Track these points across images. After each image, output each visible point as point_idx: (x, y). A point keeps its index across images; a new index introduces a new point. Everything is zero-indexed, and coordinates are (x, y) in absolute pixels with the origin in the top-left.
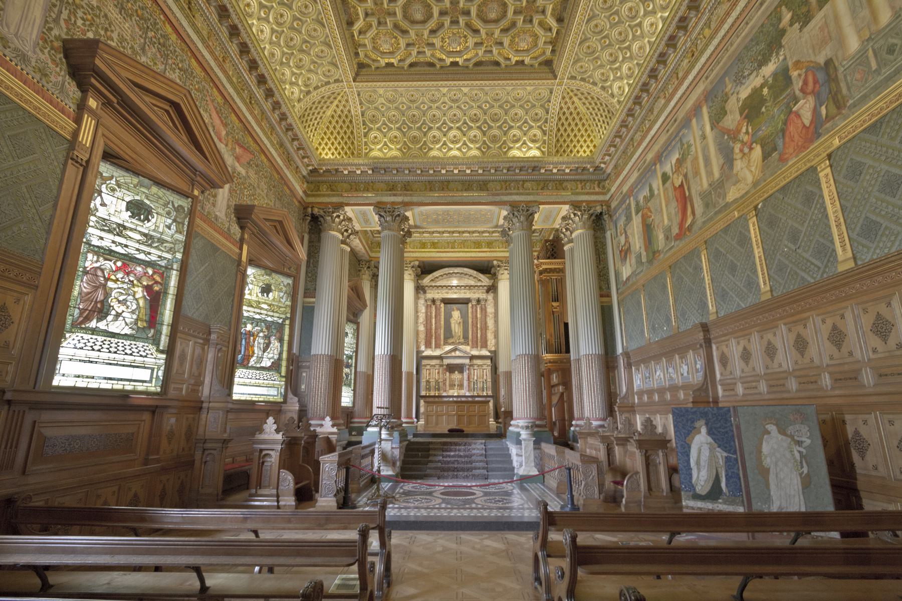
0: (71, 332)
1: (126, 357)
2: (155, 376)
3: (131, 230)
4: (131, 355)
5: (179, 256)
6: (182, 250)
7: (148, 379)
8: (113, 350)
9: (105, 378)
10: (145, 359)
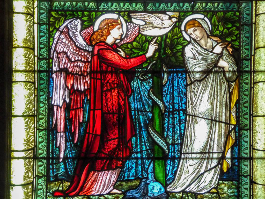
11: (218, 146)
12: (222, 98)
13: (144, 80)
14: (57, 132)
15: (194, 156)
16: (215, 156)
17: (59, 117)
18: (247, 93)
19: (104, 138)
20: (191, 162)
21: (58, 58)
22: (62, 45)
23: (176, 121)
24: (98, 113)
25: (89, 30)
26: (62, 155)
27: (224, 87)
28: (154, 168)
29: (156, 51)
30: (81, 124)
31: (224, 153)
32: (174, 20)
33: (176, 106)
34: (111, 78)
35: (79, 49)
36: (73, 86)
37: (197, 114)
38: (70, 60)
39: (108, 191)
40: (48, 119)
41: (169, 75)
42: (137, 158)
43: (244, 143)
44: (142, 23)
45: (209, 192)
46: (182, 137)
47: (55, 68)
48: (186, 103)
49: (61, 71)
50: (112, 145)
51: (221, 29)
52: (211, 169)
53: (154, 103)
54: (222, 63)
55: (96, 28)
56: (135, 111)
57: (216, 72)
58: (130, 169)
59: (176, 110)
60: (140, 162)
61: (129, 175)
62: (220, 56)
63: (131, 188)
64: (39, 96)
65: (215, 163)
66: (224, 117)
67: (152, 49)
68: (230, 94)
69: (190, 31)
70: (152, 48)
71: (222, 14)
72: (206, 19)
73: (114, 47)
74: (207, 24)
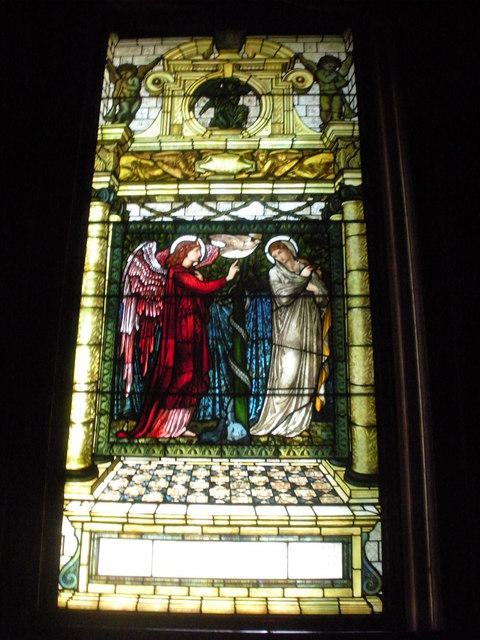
0: (109, 458)
2: (357, 562)
3: (216, 152)
4: (272, 502)
5: (353, 179)
6: (356, 161)
7: (338, 574)
9: (212, 583)
10: (320, 511)
11: (309, 380)
12: (311, 325)
13: (224, 305)
14: (124, 364)
15: (280, 392)
16: (306, 392)
17: (127, 345)
18: (340, 319)
19: (177, 371)
20: (277, 399)
21: (130, 282)
22: (134, 268)
23: (260, 352)
24: (171, 342)
25: (165, 253)
26: (128, 389)
27: (314, 313)
28: (234, 407)
29: (237, 274)
30: (151, 355)
31: (316, 389)
32: (257, 242)
33: (260, 334)
34: (187, 304)
35: (153, 272)
36: (144, 312)
37: (284, 343)
38: (142, 285)
39: (180, 432)
40: (116, 348)
41: (251, 300)
42: (214, 395)
43: (339, 377)
44: (222, 245)
45: (300, 435)
46: (267, 370)
47: (126, 292)
48: (271, 331)
49: (131, 296)
50: (187, 377)
51: (308, 251)
52: (301, 408)
53: (234, 330)
54: (311, 287)
55: (172, 251)
56: (213, 340)
57: (305, 297)
58: (206, 408)
59: (259, 339)
60: (218, 399)
61: (205, 414)
62: (309, 279)
63: (207, 430)
64: (107, 323)
65: (306, 400)
66: (315, 347)
67: (233, 271)
68: (322, 321)
69: (275, 253)
70: (233, 271)
71: (309, 235)
72: (292, 240)
73: (191, 270)
74: (294, 245)
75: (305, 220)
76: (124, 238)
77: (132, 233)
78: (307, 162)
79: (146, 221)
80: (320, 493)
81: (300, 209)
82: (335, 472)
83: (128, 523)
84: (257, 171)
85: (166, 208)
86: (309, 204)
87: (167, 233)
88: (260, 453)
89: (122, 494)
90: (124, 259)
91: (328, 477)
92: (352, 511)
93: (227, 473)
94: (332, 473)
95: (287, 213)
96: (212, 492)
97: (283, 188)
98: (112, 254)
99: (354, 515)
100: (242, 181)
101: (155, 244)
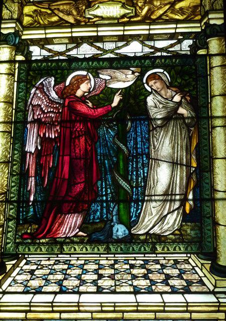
1: (141, 298)
4: (151, 292)
8: (106, 283)
10: (190, 298)
11: (180, 188)
12: (182, 142)
13: (110, 127)
14: (29, 177)
15: (157, 198)
16: (178, 197)
17: (31, 162)
18: (206, 137)
19: (71, 183)
20: (154, 204)
21: (33, 110)
22: (36, 99)
23: (140, 165)
24: (67, 158)
25: (61, 86)
26: (32, 199)
27: (183, 133)
28: (119, 210)
29: (120, 101)
30: (50, 169)
31: (186, 195)
32: (137, 74)
33: (140, 150)
34: (79, 127)
35: (52, 102)
36: (44, 134)
37: (159, 158)
38: (43, 112)
39: (74, 233)
40: (21, 165)
41: (132, 123)
42: (102, 201)
43: (205, 185)
44: (108, 78)
45: (172, 234)
46: (145, 179)
47: (30, 119)
48: (148, 148)
49: (34, 121)
50: (79, 188)
51: (179, 81)
52: (174, 211)
53: (119, 148)
54: (181, 111)
55: (67, 83)
56: (100, 156)
57: (176, 119)
58: (95, 212)
59: (139, 154)
60: (105, 204)
61: (94, 217)
62: (179, 104)
63: (96, 231)
64: (14, 144)
65: (177, 204)
66: (185, 159)
67: (117, 99)
68: (190, 139)
69: (151, 83)
70: (117, 99)
71: (180, 68)
72: (165, 72)
73: (83, 99)
74: (167, 76)
75: (176, 55)
76: (28, 74)
77: (34, 71)
78: (178, 6)
79: (46, 59)
80: (190, 283)
81: (172, 46)
82: (202, 264)
83: (30, 311)
84: (136, 15)
85: (62, 48)
86: (180, 42)
87: (63, 69)
88: (140, 249)
89: (26, 286)
90: (28, 92)
91: (197, 269)
92: (217, 298)
93: (112, 266)
94: (200, 265)
95: (161, 50)
96: (100, 283)
97: (158, 29)
98: (18, 88)
99: (219, 302)
100: (124, 24)
101: (53, 78)
